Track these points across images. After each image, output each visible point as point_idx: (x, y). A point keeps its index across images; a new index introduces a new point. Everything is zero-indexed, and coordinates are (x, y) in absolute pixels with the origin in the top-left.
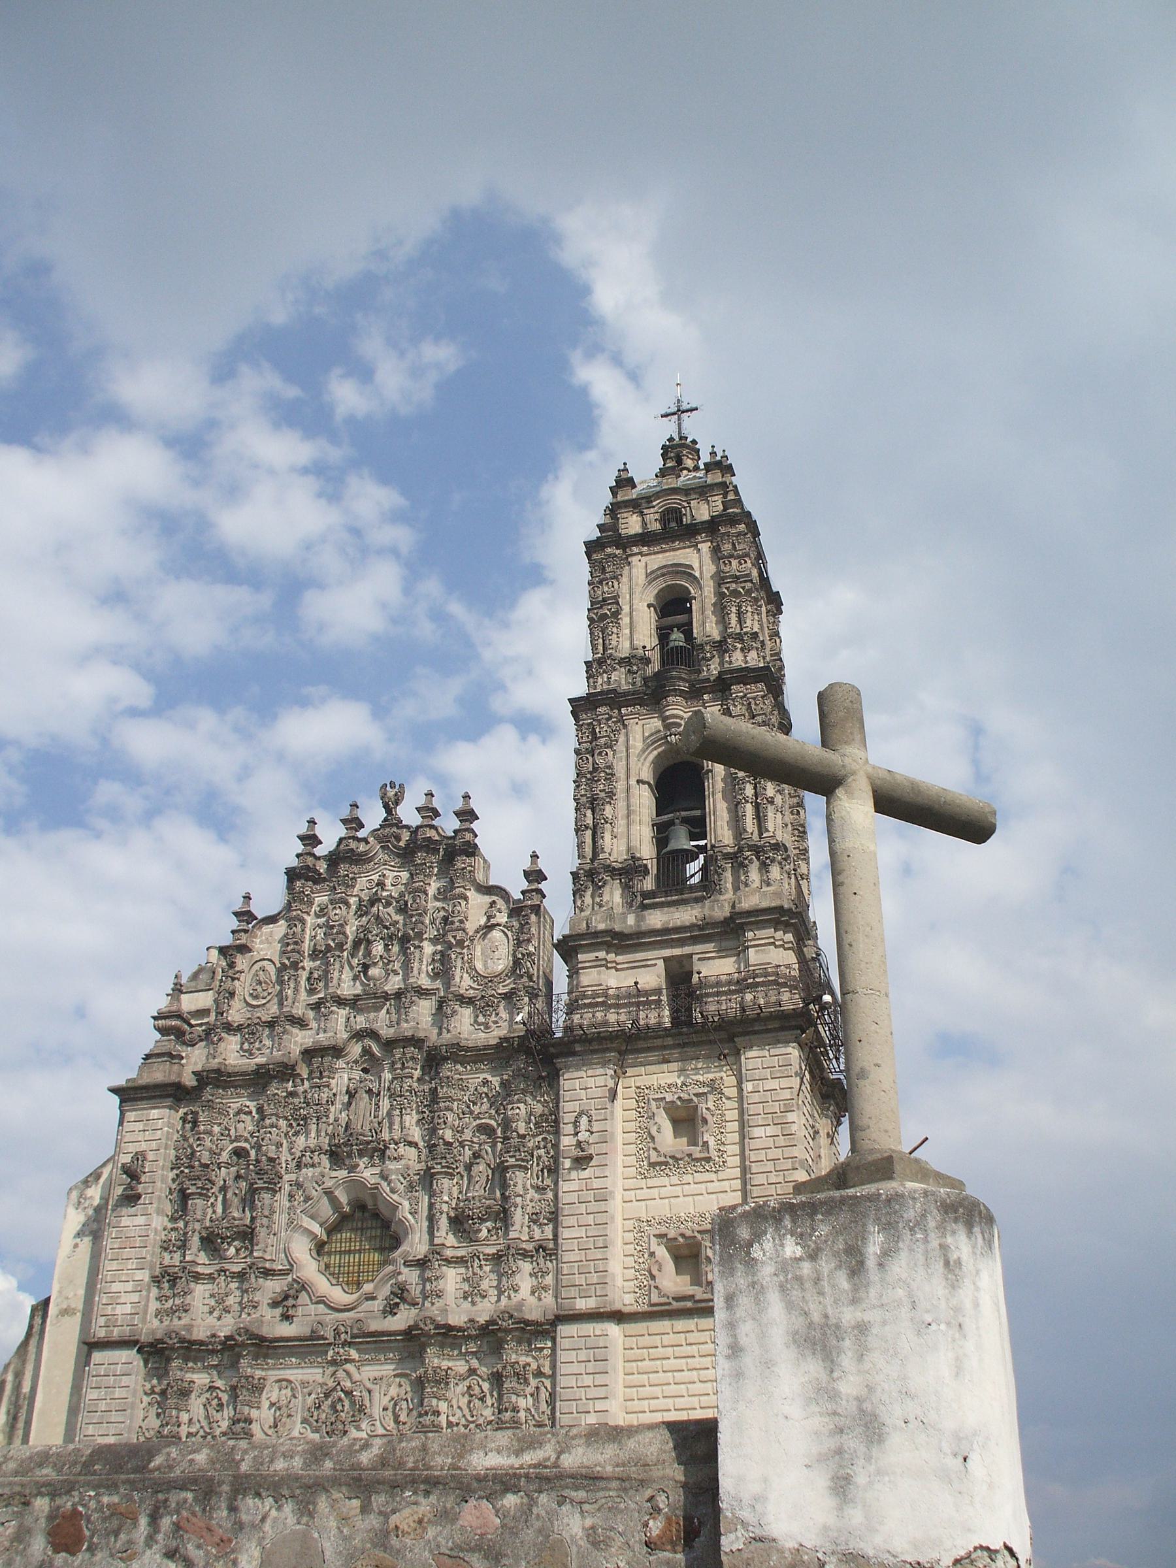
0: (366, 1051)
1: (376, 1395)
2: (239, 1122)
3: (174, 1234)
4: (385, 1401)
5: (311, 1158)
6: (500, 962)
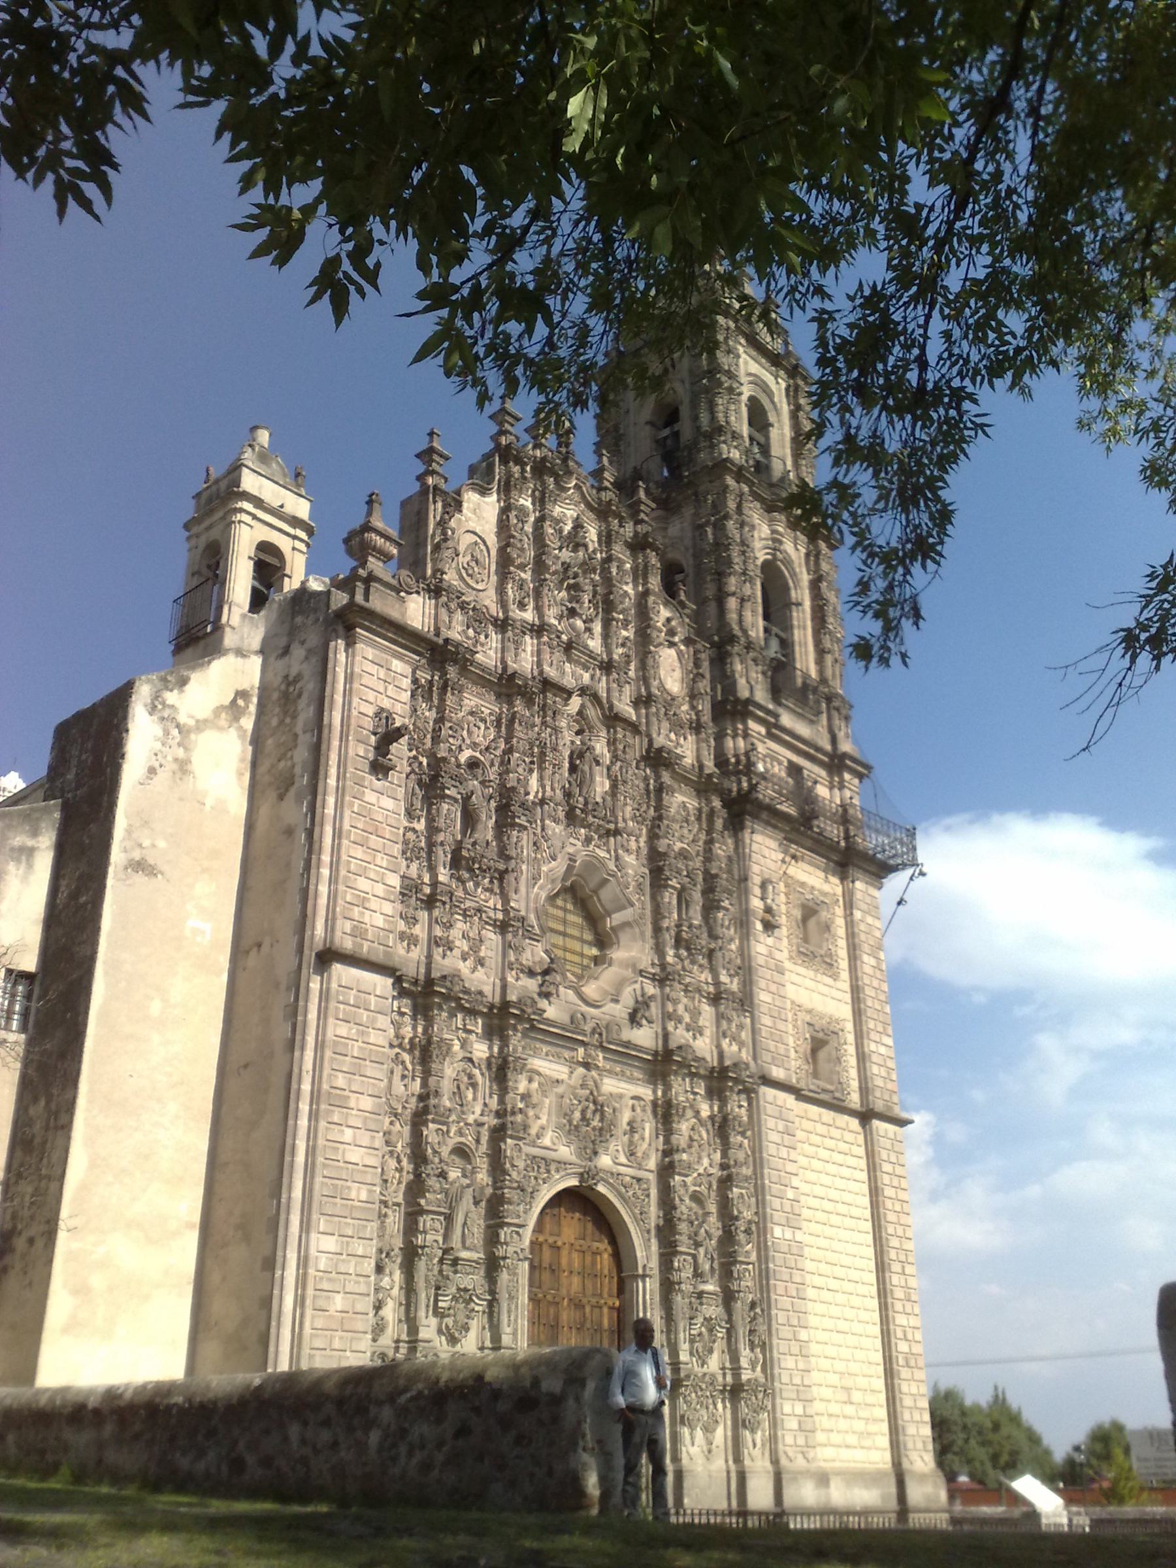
0: (580, 713)
3: (411, 836)
4: (625, 1127)
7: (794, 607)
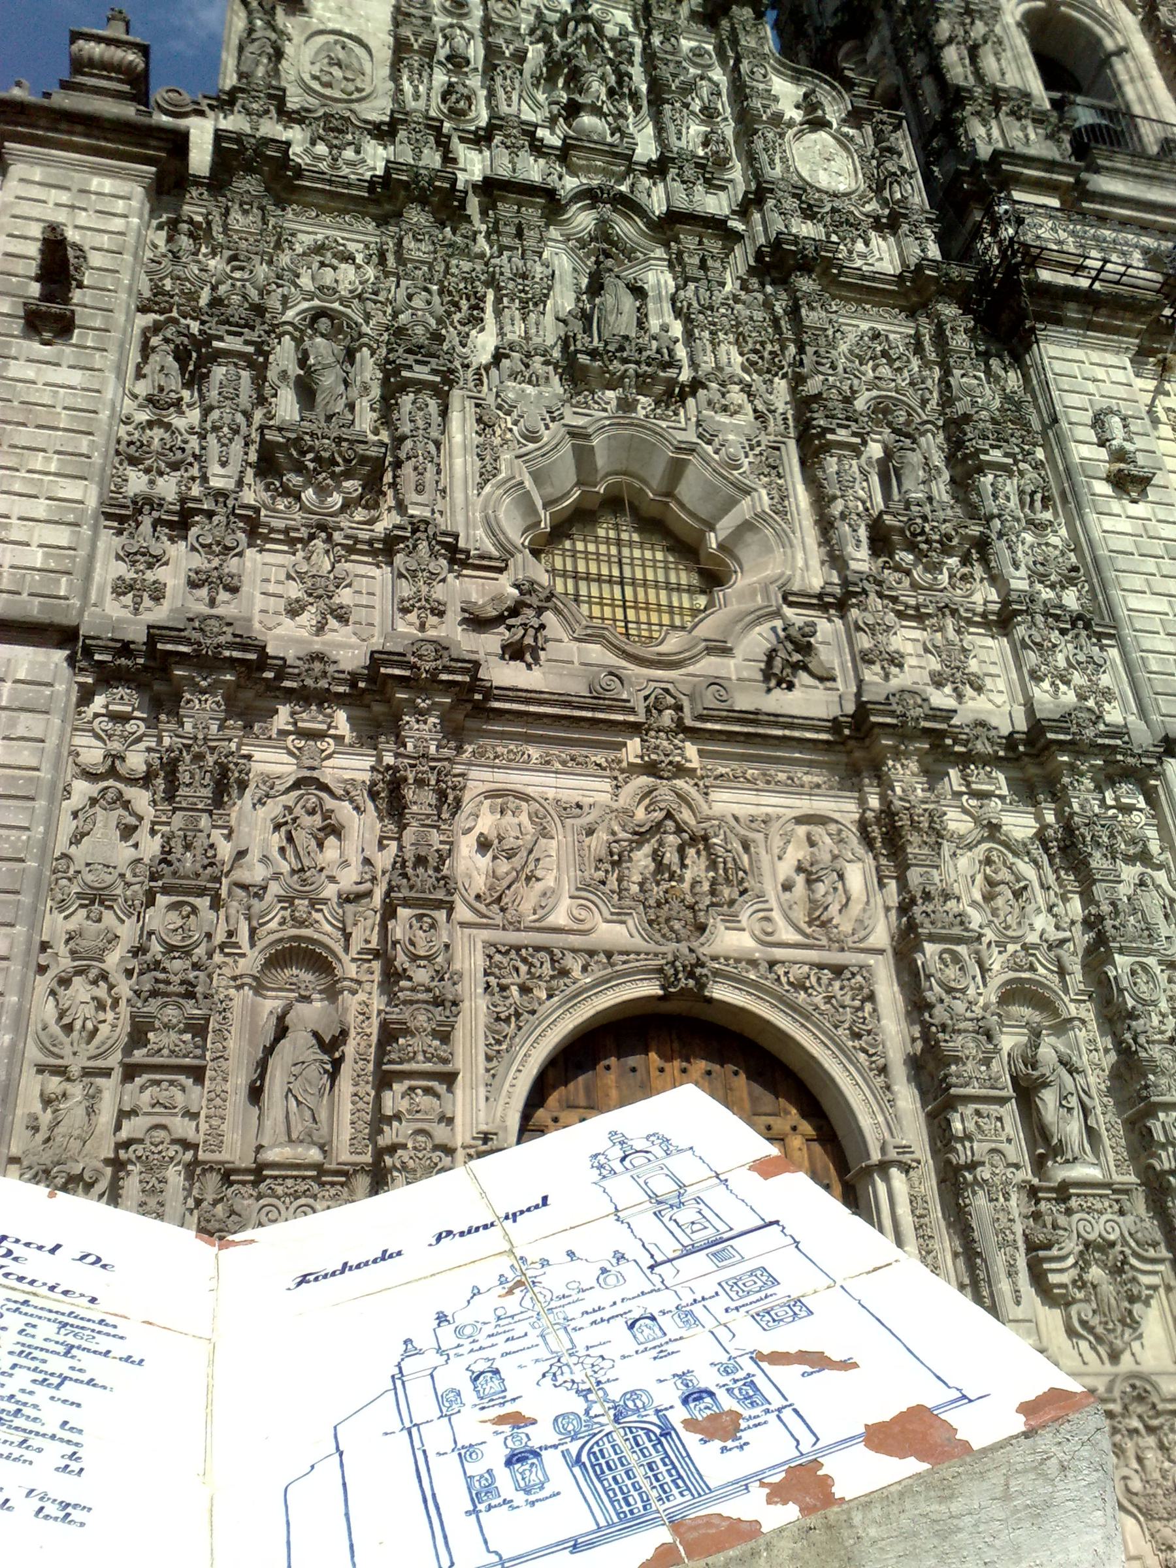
1: (765, 858)
2: (322, 264)
4: (786, 869)
5: (527, 366)
6: (841, 179)
7: (1114, 59)
